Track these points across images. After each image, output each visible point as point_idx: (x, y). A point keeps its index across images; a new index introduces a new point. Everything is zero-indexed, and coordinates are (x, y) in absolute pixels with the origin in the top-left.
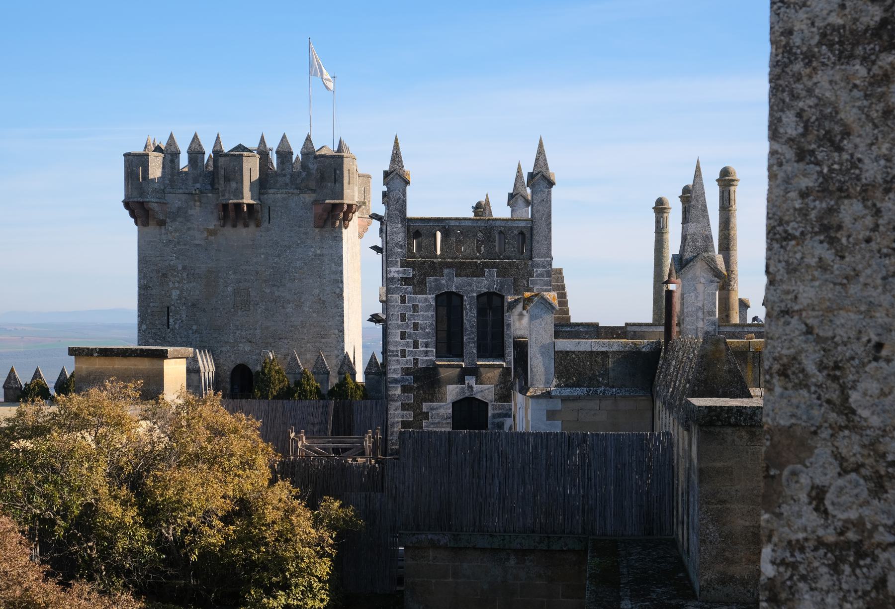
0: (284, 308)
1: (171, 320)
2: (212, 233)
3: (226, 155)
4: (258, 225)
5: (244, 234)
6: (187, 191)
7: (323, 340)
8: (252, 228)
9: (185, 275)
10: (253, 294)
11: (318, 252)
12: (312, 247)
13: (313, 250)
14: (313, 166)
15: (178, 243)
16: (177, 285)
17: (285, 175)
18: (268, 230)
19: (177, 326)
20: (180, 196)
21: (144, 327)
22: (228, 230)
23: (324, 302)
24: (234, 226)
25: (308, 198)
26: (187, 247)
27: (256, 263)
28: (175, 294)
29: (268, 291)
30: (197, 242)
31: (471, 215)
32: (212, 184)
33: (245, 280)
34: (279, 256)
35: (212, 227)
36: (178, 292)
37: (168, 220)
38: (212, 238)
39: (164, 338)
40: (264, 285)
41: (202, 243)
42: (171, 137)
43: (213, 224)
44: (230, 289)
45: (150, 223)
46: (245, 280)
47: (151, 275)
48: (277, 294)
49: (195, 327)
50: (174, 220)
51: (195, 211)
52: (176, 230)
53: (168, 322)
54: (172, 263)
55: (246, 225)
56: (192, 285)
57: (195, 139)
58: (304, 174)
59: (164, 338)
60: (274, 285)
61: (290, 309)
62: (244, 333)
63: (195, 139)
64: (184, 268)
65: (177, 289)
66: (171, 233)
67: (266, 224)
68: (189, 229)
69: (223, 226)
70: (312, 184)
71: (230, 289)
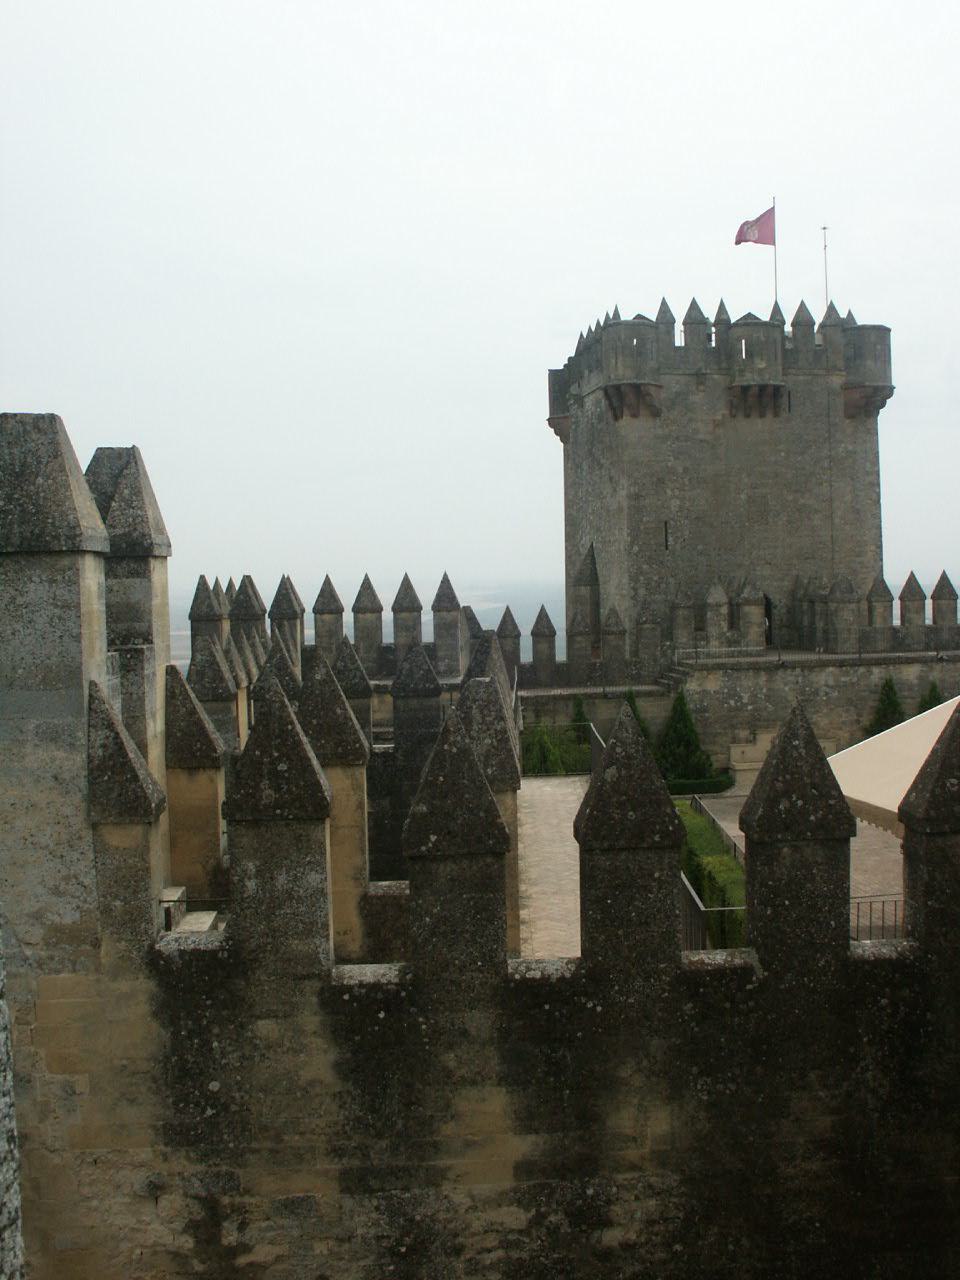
0: (809, 519)
1: (670, 539)
2: (717, 425)
3: (737, 324)
4: (776, 415)
5: (757, 428)
6: (688, 372)
7: (858, 559)
11: (850, 448)
12: (842, 442)
13: (843, 445)
14: (839, 338)
16: (677, 492)
19: (678, 547)
20: (678, 378)
21: (636, 548)
23: (858, 512)
24: (748, 416)
28: (675, 504)
30: (701, 436)
35: (719, 417)
36: (678, 503)
39: (662, 563)
42: (850, 312)
43: (722, 412)
45: (642, 412)
48: (802, 501)
49: (700, 547)
51: (697, 398)
53: (667, 541)
54: (670, 464)
55: (762, 415)
59: (662, 563)
61: (817, 520)
62: (761, 552)
64: (686, 470)
65: (677, 498)
67: (784, 415)
68: (691, 420)
69: (734, 416)
70: (841, 364)
71: (743, 496)
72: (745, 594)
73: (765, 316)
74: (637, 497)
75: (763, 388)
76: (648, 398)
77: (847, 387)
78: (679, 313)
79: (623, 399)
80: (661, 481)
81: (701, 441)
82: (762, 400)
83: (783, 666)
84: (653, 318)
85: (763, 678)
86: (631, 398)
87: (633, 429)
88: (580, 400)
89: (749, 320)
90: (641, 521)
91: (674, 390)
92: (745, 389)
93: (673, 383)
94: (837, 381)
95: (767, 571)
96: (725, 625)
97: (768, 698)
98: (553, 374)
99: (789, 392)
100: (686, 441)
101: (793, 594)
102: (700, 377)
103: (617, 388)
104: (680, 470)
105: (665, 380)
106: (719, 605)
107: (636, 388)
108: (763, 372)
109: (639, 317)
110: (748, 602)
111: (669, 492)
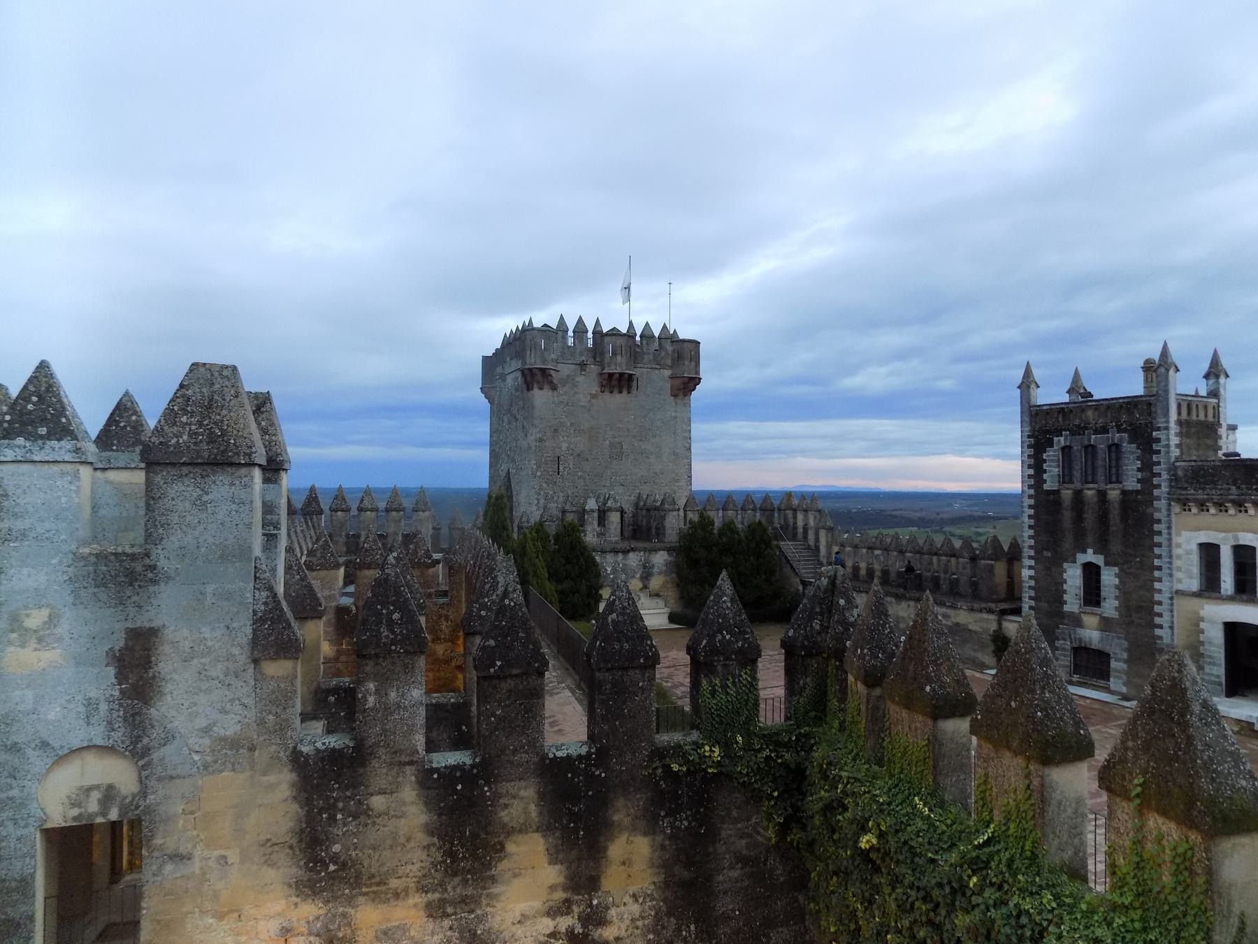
2: (594, 396)
3: (607, 334)
5: (617, 400)
22: (607, 394)
25: (667, 373)
28: (565, 445)
31: (1066, 398)
32: (594, 358)
38: (594, 401)
43: (595, 389)
50: (563, 386)
51: (580, 379)
52: (566, 393)
57: (580, 320)
63: (580, 320)
64: (572, 424)
67: (634, 391)
70: (669, 362)
72: (609, 504)
73: (624, 329)
74: (541, 440)
75: (621, 375)
77: (671, 377)
78: (571, 324)
79: (535, 378)
80: (556, 430)
82: (620, 383)
83: (633, 550)
84: (554, 325)
85: (620, 557)
86: (539, 377)
87: (541, 397)
88: (503, 377)
89: (614, 333)
92: (611, 375)
93: (566, 370)
94: (667, 373)
95: (620, 490)
96: (596, 523)
97: (623, 570)
98: (485, 359)
101: (636, 505)
102: (583, 366)
103: (531, 370)
105: (560, 367)
106: (593, 511)
107: (543, 370)
108: (619, 366)
109: (545, 325)
110: (610, 510)
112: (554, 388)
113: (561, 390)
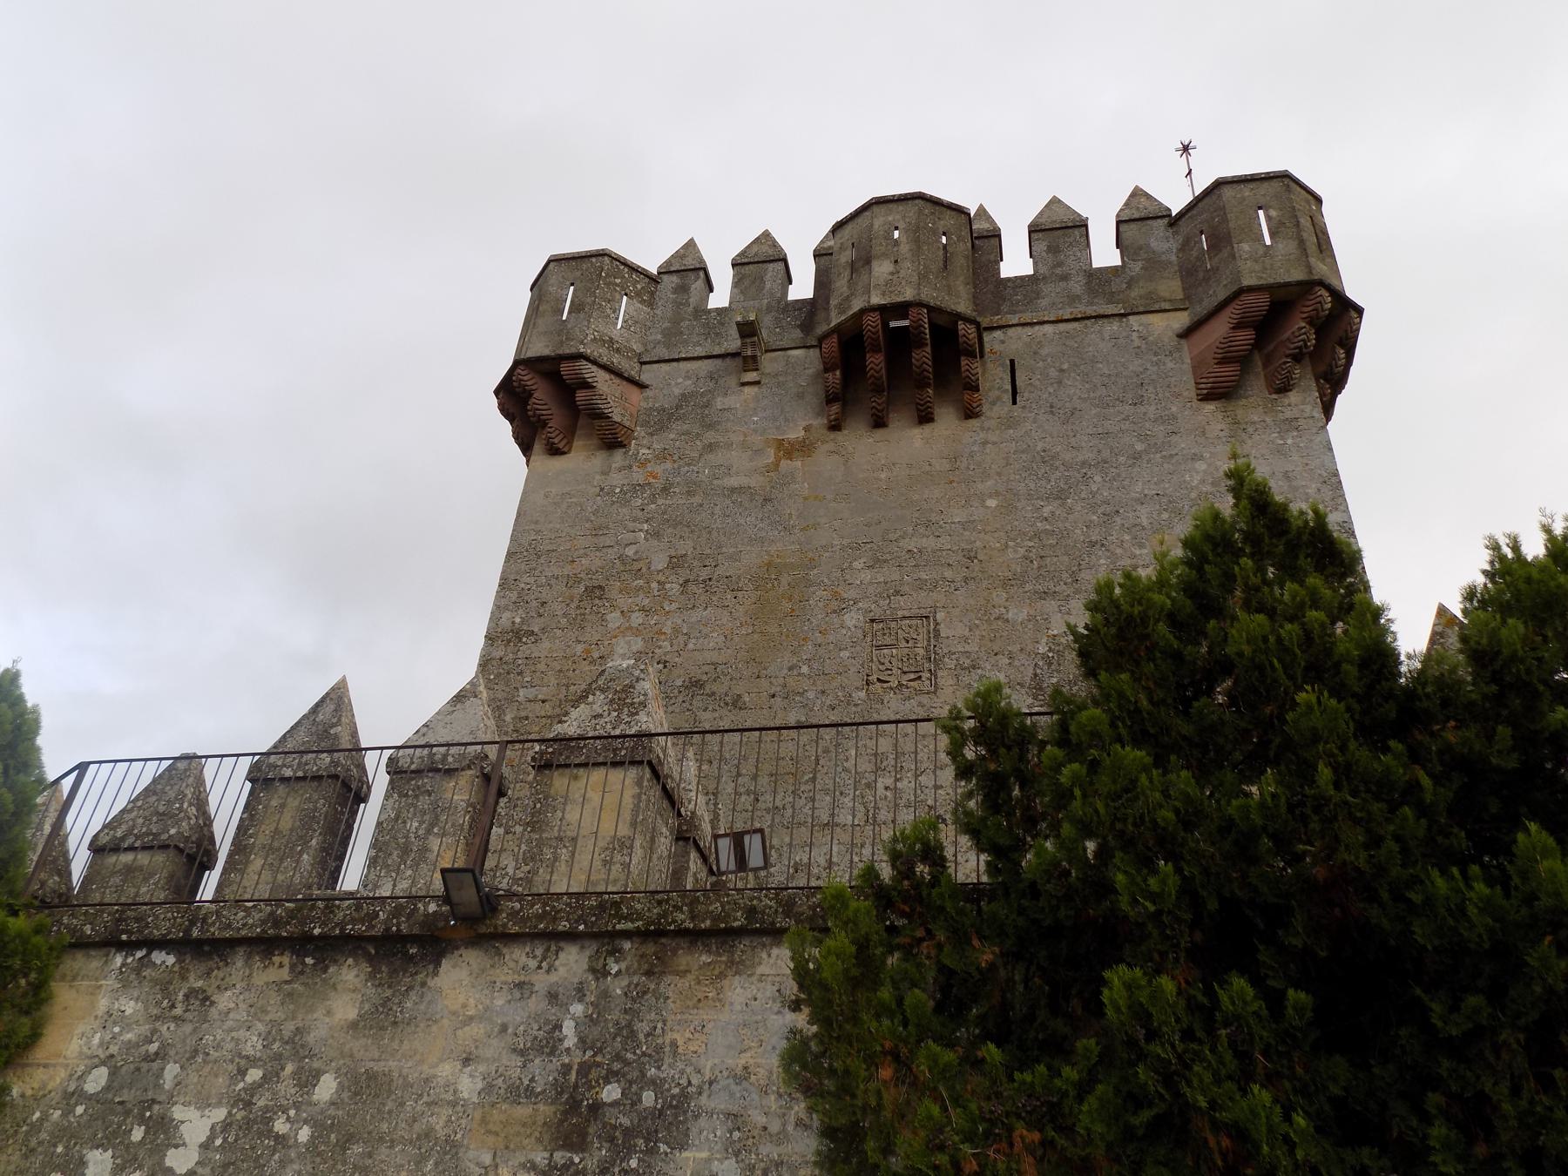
2: (789, 450)
8: (947, 422)
9: (674, 588)
10: (952, 630)
12: (1196, 457)
13: (1201, 466)
15: (665, 490)
16: (637, 619)
17: (1065, 278)
18: (1011, 423)
26: (697, 500)
27: (964, 525)
29: (1017, 614)
30: (734, 482)
33: (920, 585)
34: (1060, 496)
37: (639, 431)
40: (999, 596)
41: (755, 482)
44: (852, 619)
46: (920, 585)
47: (546, 594)
52: (663, 456)
54: (630, 551)
55: (925, 418)
56: (695, 616)
58: (1136, 267)
60: (1044, 595)
64: (676, 563)
65: (637, 632)
66: (643, 465)
68: (710, 448)
69: (835, 427)
71: (852, 619)
76: (581, 395)
80: (596, 592)
81: (733, 490)
90: (511, 700)
91: (677, 391)
99: (1012, 362)
100: (690, 493)
104: (660, 562)
111: (614, 619)
112: (613, 441)
113: (643, 446)
